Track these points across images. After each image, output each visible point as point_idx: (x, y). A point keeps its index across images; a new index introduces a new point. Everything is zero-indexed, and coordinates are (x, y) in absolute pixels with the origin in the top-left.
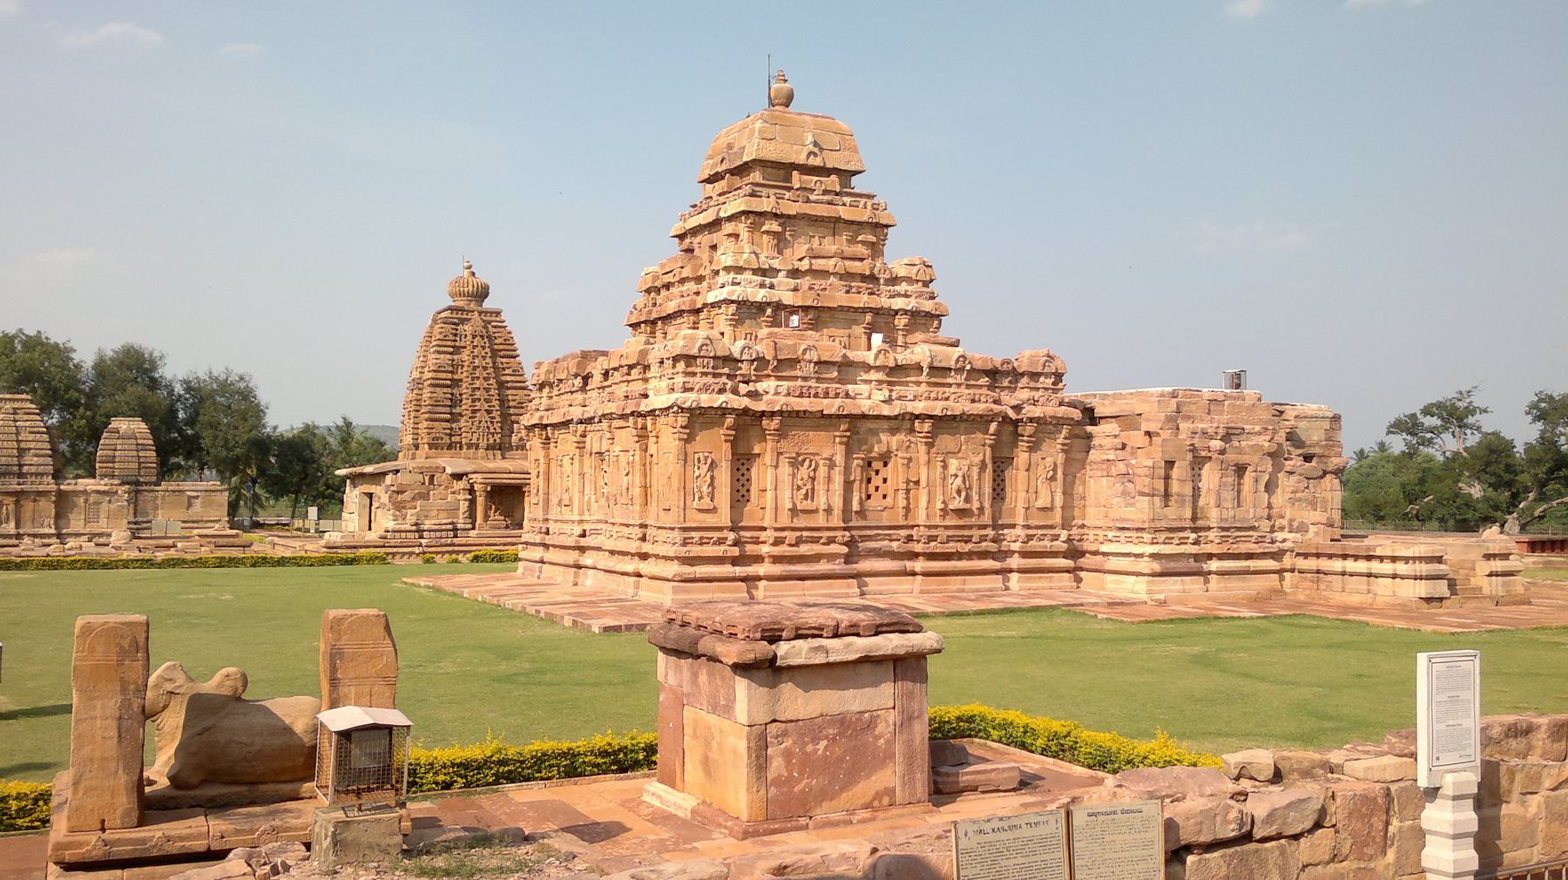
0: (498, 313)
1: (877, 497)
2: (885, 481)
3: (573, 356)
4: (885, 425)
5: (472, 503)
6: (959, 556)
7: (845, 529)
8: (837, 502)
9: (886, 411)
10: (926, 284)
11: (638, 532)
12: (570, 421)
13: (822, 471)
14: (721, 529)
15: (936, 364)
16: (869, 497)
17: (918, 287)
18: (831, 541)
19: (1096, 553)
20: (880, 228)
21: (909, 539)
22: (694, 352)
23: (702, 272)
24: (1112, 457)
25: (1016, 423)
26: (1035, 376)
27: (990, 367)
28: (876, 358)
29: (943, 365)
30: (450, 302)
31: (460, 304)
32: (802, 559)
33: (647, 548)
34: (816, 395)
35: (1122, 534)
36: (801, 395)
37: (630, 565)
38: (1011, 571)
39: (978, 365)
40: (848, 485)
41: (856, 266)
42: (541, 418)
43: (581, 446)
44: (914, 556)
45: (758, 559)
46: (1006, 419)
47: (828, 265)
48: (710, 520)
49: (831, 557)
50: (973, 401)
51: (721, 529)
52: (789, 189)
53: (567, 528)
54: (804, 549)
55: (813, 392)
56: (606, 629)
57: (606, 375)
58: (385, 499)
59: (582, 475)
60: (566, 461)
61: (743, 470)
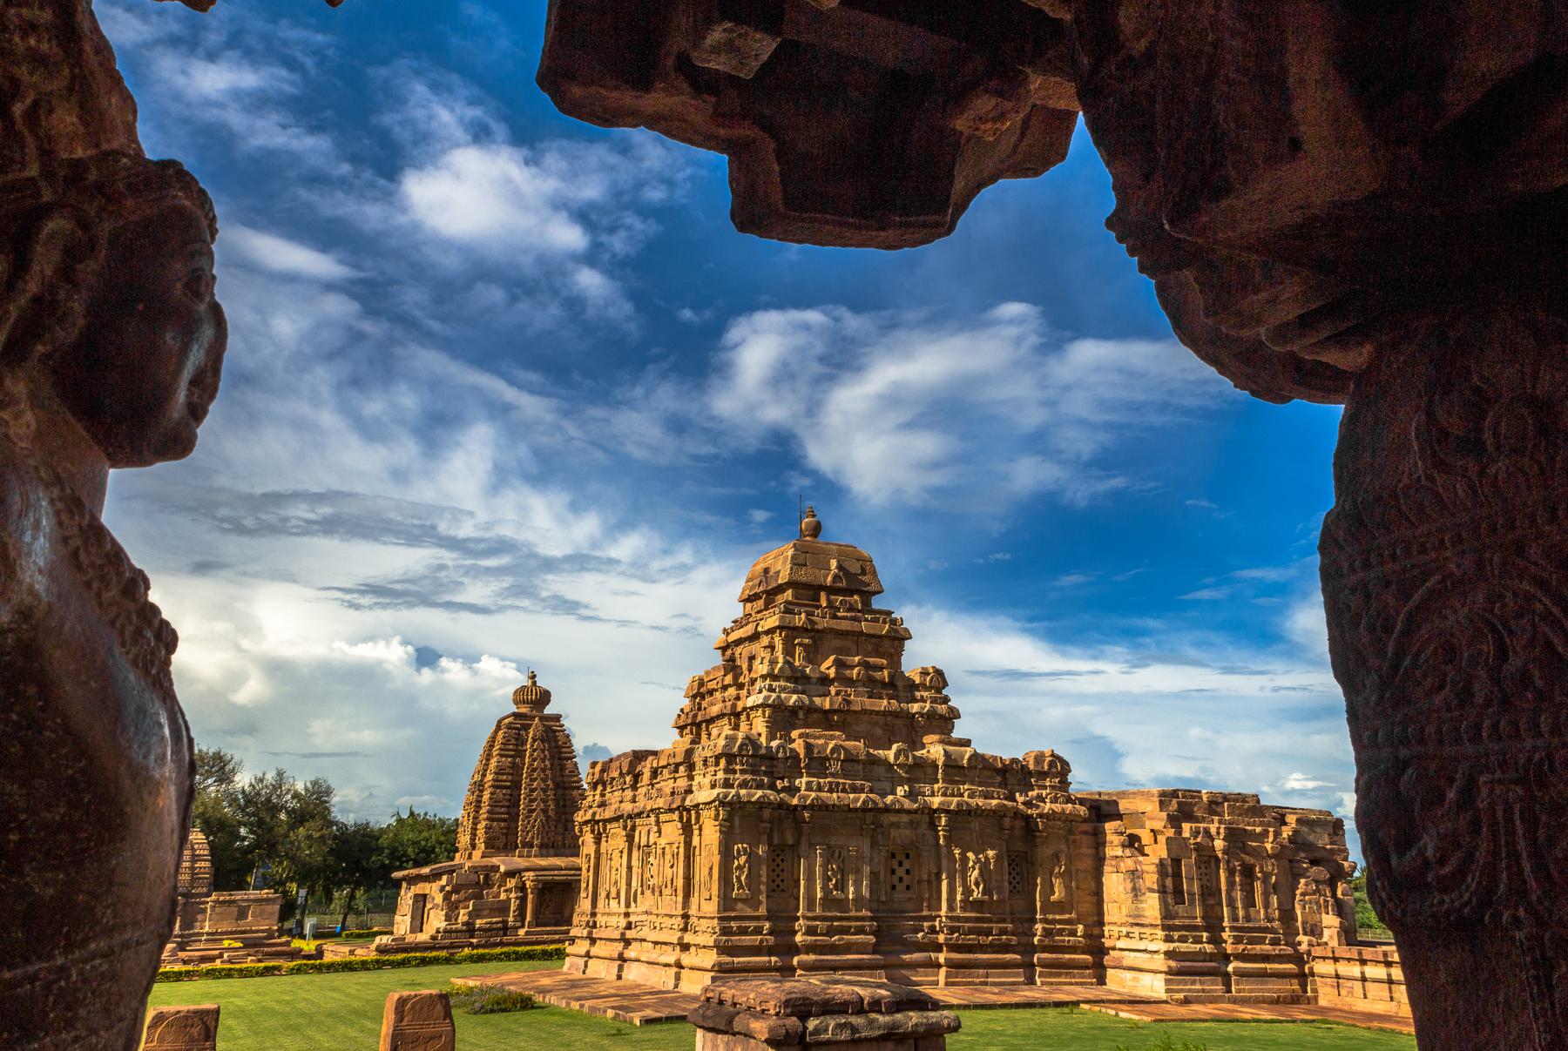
0: (557, 718)
1: (900, 887)
2: (908, 872)
3: (625, 755)
4: (905, 818)
5: (523, 900)
6: (982, 948)
7: (872, 919)
8: (865, 892)
9: (907, 804)
10: (939, 691)
12: (621, 816)
14: (758, 918)
16: (894, 887)
17: (932, 693)
18: (860, 931)
19: (1114, 949)
23: (741, 679)
24: (1119, 853)
26: (1043, 775)
30: (514, 709)
31: (524, 710)
32: (834, 949)
34: (844, 790)
35: (1136, 930)
36: (831, 791)
42: (594, 814)
43: (630, 838)
51: (758, 918)
52: (818, 607)
56: (648, 1022)
57: (655, 773)
58: (439, 898)
59: (630, 868)
60: (616, 854)
61: (778, 861)
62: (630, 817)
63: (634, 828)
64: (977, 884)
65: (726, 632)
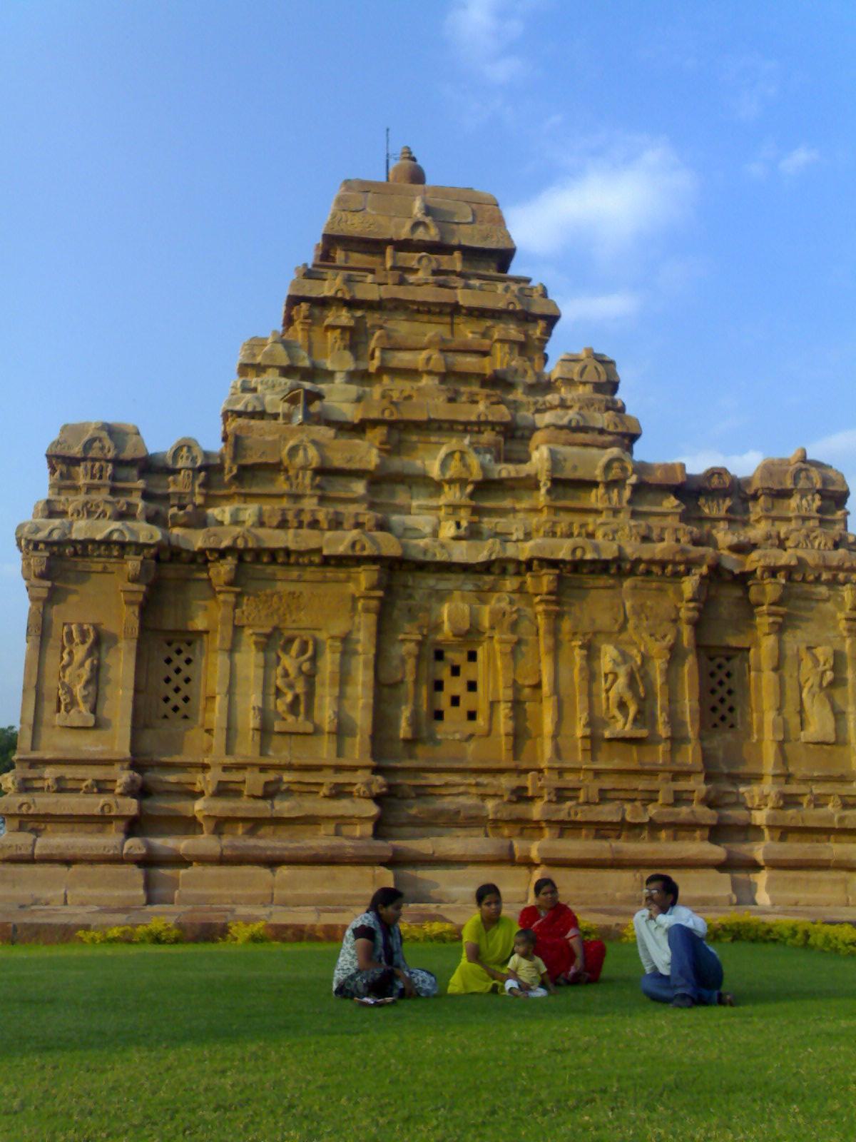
8: (361, 717)
9: (462, 553)
13: (329, 662)
15: (568, 474)
16: (439, 715)
21: (520, 796)
22: (76, 451)
25: (743, 579)
27: (680, 479)
28: (444, 465)
29: (580, 474)
34: (314, 524)
36: (283, 524)
38: (755, 866)
39: (658, 477)
40: (384, 691)
41: (468, 363)
44: (527, 827)
45: (189, 825)
46: (717, 573)
47: (417, 359)
48: (89, 745)
49: (341, 821)
50: (646, 539)
54: (283, 807)
55: (306, 518)
64: (622, 705)
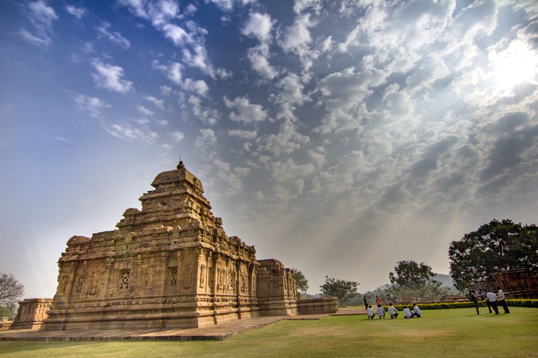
11: (160, 300)
20: (209, 208)
33: (167, 306)
37: (160, 315)
42: (78, 258)
53: (95, 304)
62: (113, 257)
63: (113, 263)
65: (144, 194)
